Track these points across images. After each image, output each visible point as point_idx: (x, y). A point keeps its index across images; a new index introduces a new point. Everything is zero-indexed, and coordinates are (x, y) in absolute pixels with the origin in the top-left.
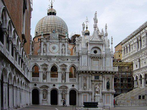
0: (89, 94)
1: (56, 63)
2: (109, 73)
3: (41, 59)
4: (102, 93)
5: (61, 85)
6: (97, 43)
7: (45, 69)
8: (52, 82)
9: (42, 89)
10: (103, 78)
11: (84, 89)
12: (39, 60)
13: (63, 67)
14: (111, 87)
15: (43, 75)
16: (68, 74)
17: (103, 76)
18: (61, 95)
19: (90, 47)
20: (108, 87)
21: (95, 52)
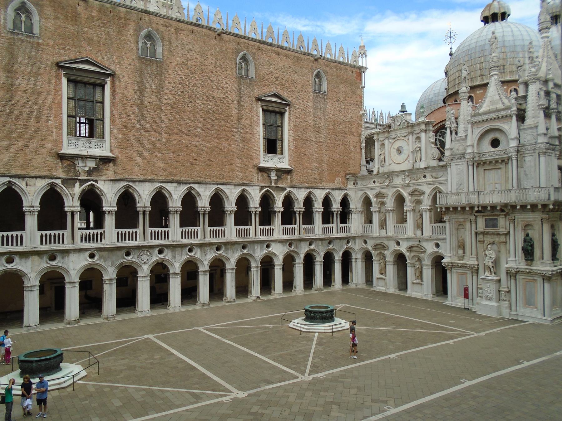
0: (469, 273)
1: (403, 187)
2: (523, 207)
3: (374, 182)
4: (507, 273)
5: (411, 243)
6: (492, 116)
7: (383, 204)
8: (396, 235)
9: (377, 252)
10: (512, 225)
11: (459, 257)
12: (372, 185)
13: (416, 198)
14: (537, 253)
15: (380, 219)
16: (428, 213)
17: (511, 217)
18: (413, 269)
19: (473, 135)
20: (528, 253)
21: (495, 143)
